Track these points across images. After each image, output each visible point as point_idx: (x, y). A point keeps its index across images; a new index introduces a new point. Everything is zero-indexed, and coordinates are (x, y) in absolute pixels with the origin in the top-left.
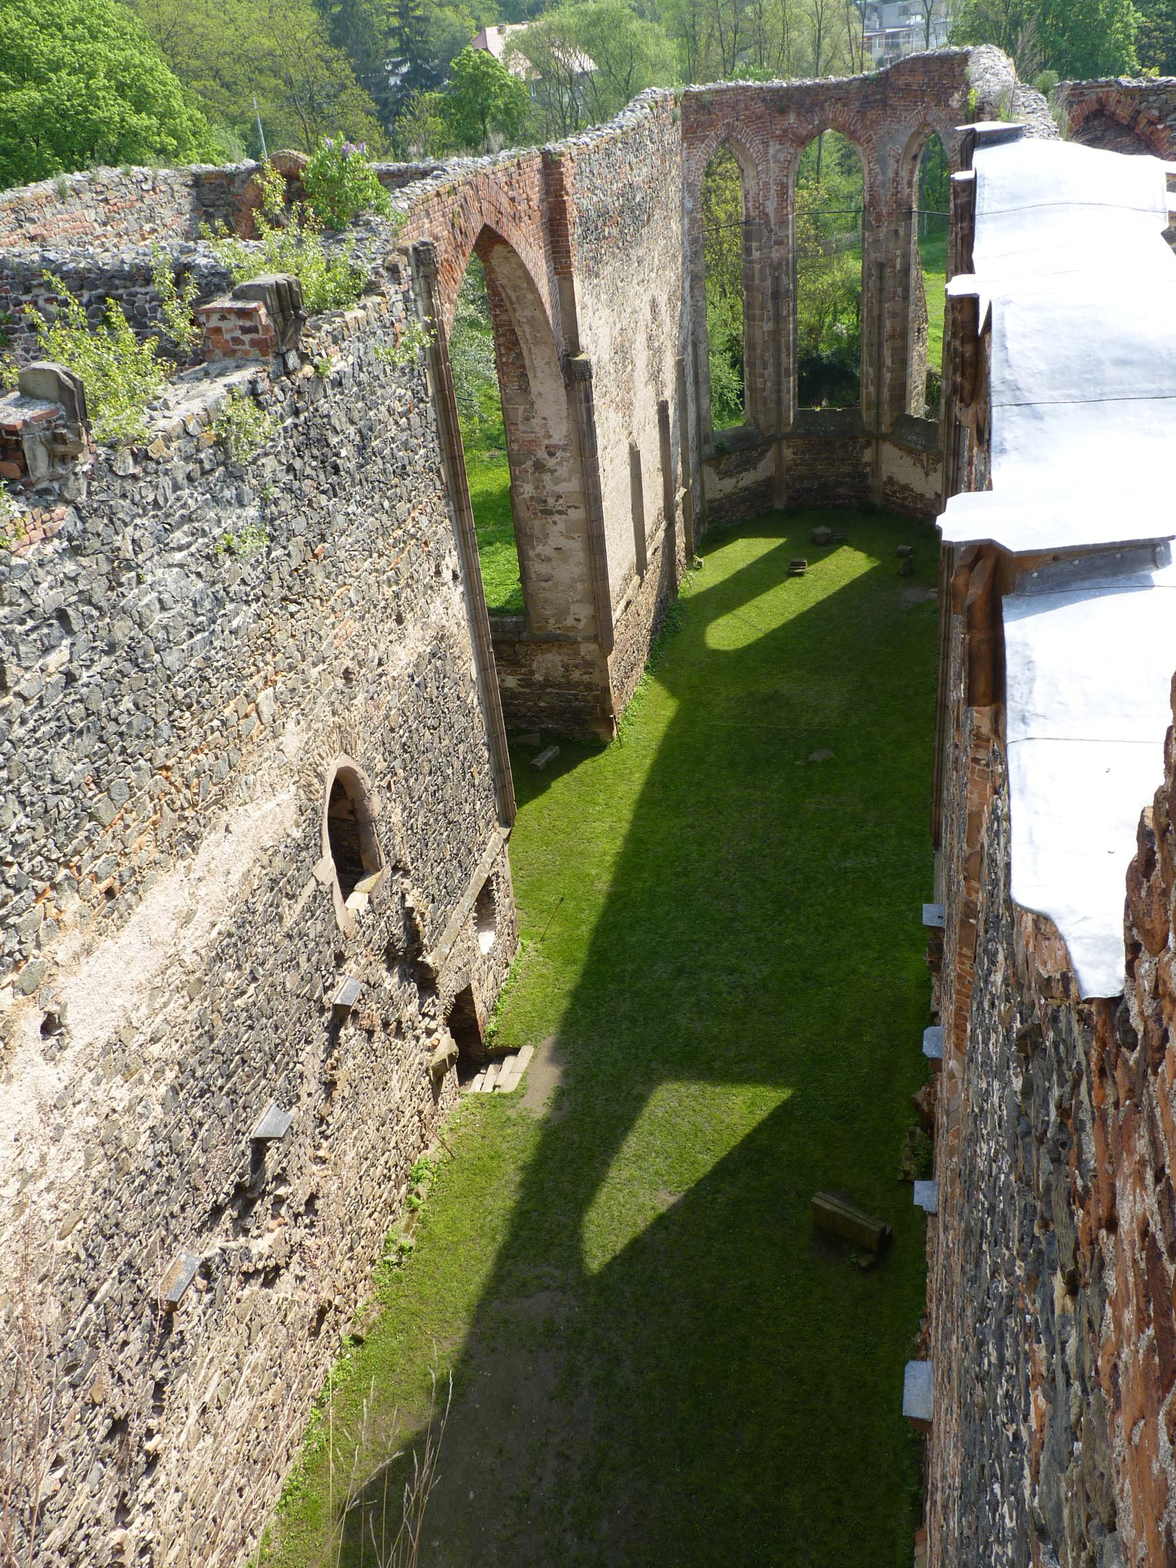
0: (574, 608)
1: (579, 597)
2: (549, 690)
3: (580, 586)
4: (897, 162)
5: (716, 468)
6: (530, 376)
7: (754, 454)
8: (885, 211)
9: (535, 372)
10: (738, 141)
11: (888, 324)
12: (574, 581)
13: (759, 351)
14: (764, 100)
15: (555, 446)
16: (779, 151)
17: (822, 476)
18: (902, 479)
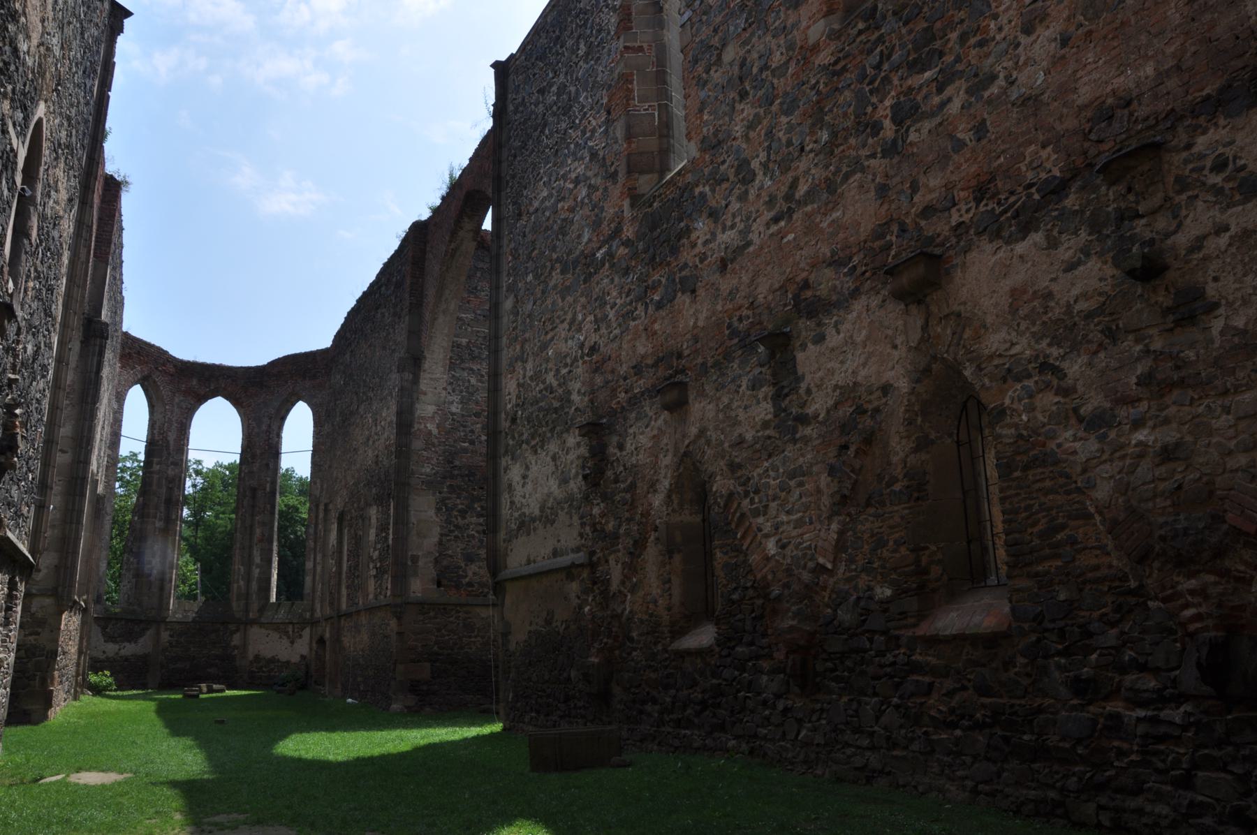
4: (270, 418)
5: (104, 629)
8: (258, 452)
10: (155, 382)
11: (258, 531)
14: (175, 366)
18: (268, 654)
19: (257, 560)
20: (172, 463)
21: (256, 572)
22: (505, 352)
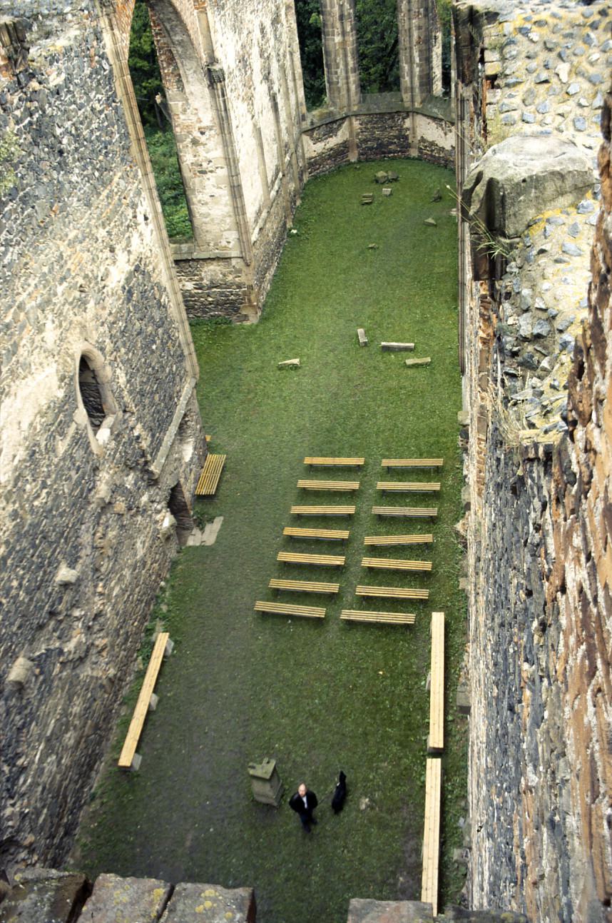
1: (228, 227)
2: (215, 290)
3: (228, 220)
5: (311, 136)
7: (335, 126)
9: (187, 78)
13: (333, 56)
17: (379, 139)
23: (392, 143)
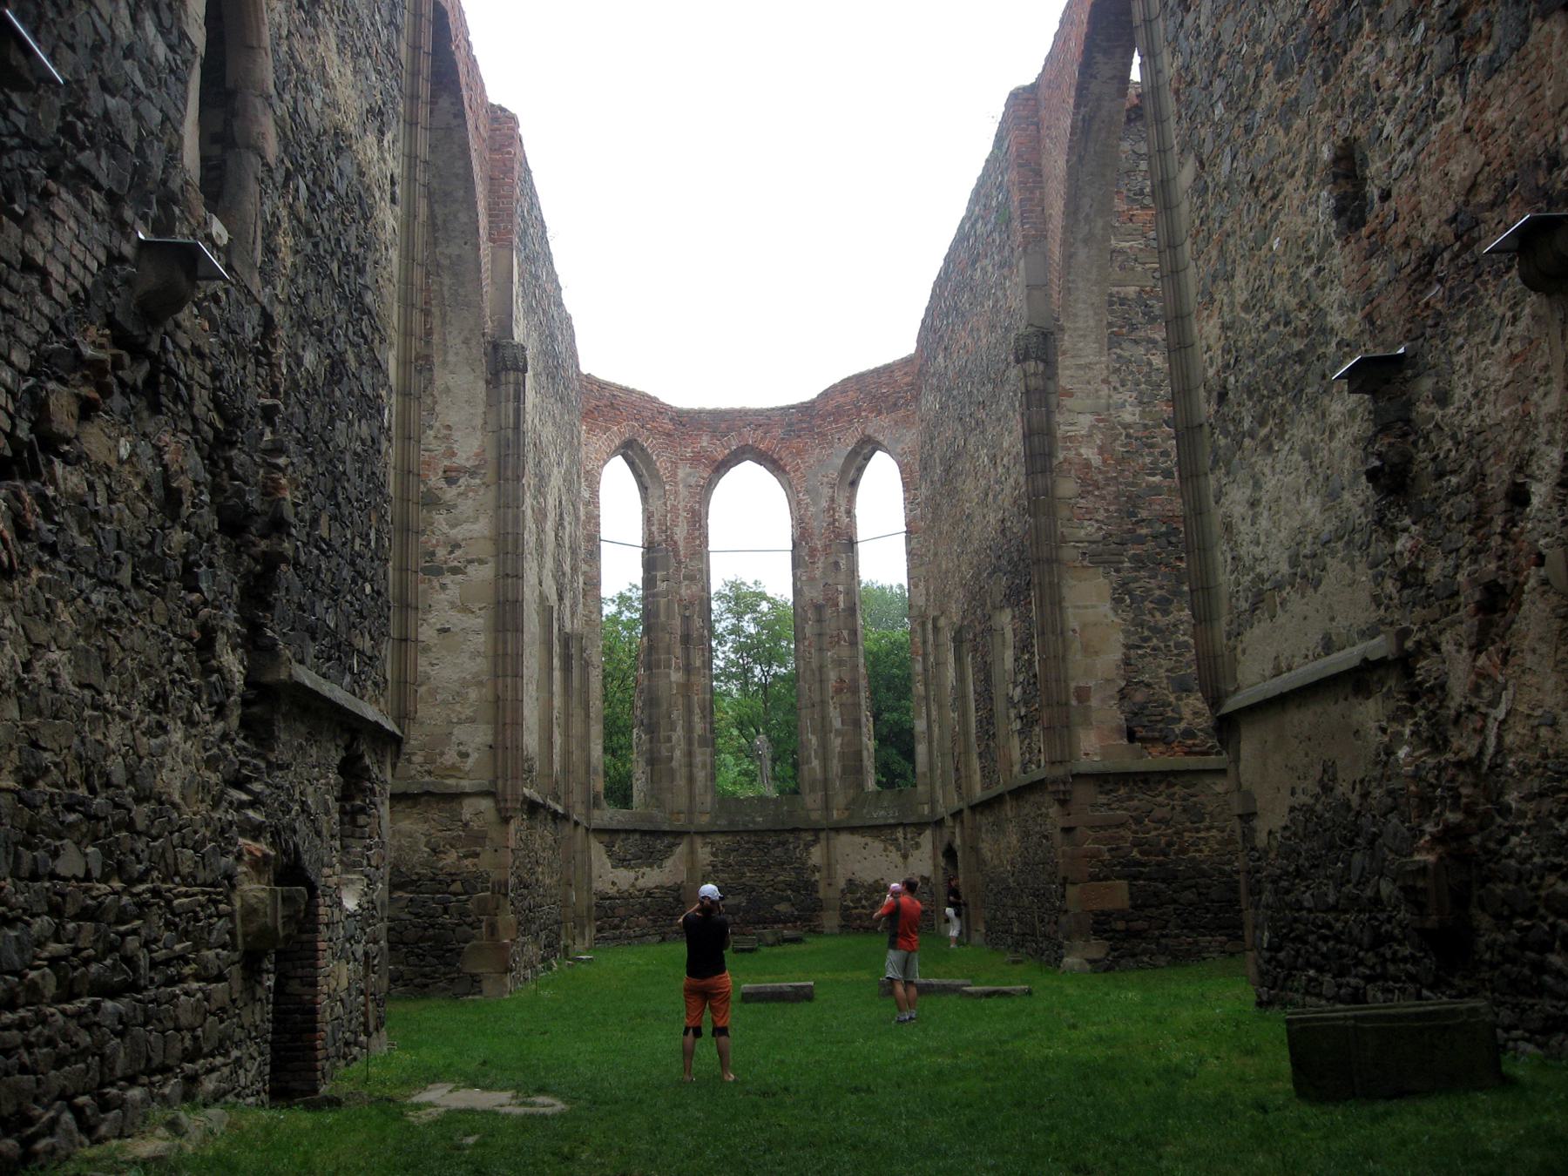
0: (459, 733)
1: (468, 712)
3: (473, 694)
5: (609, 848)
6: (437, 360)
9: (446, 353)
10: (643, 449)
11: (833, 676)
12: (464, 683)
13: (664, 707)
15: (457, 470)
16: (689, 475)
19: (837, 723)
20: (685, 578)
21: (836, 743)
22: (1192, 270)
23: (782, 899)
